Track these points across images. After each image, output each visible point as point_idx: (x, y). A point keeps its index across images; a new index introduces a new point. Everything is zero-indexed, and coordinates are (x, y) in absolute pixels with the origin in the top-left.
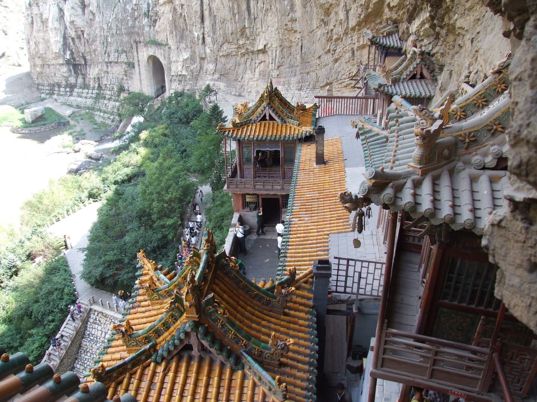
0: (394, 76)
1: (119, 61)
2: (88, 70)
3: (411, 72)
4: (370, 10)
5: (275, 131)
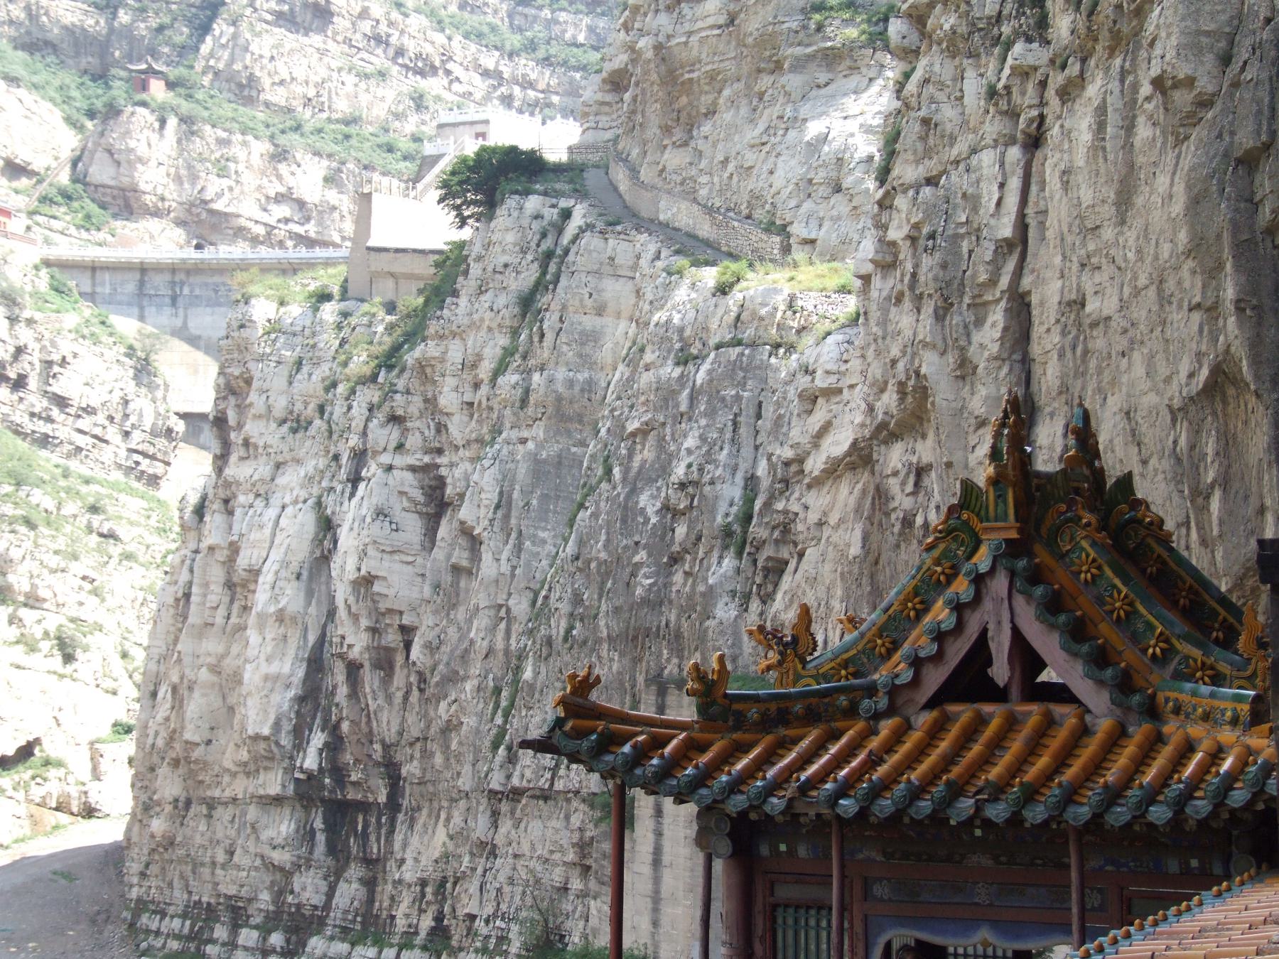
1: (559, 785)
2: (398, 838)
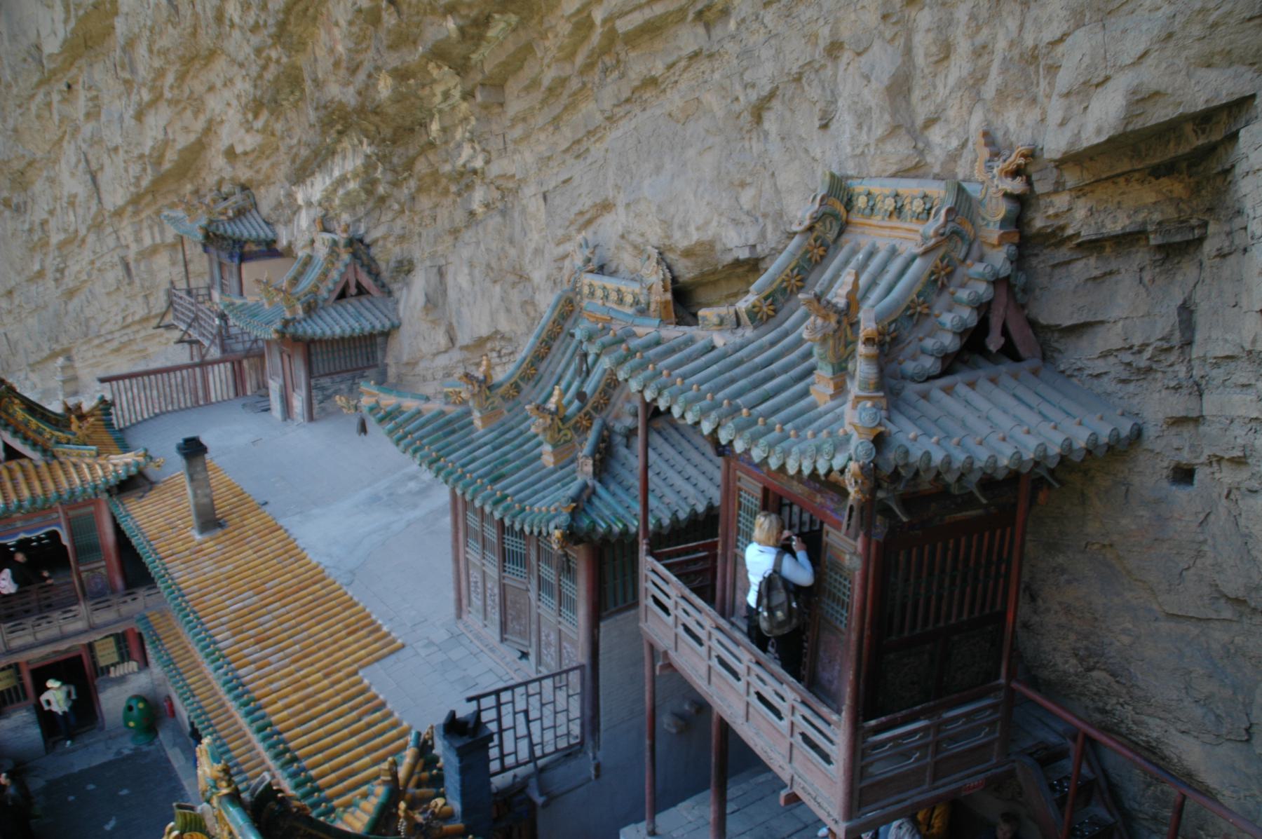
0: (303, 299)
3: (335, 283)
4: (167, 166)
5: (37, 484)
